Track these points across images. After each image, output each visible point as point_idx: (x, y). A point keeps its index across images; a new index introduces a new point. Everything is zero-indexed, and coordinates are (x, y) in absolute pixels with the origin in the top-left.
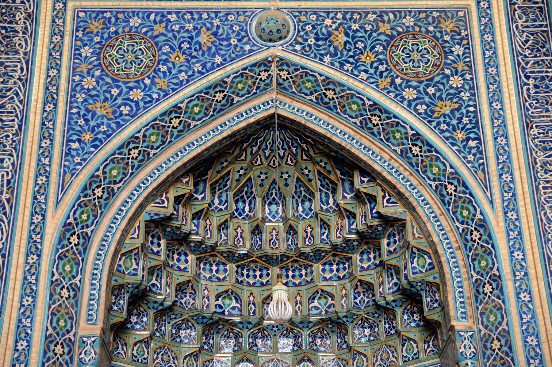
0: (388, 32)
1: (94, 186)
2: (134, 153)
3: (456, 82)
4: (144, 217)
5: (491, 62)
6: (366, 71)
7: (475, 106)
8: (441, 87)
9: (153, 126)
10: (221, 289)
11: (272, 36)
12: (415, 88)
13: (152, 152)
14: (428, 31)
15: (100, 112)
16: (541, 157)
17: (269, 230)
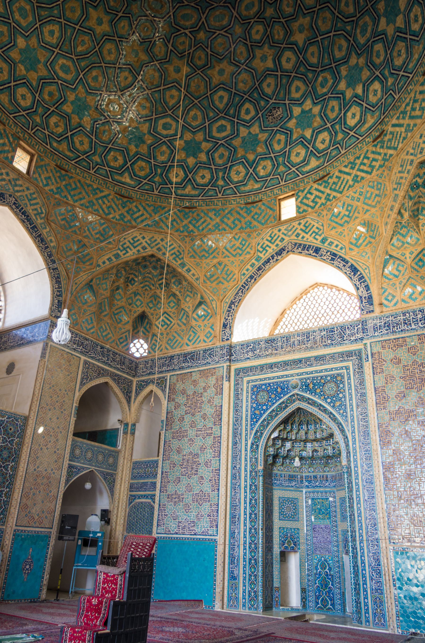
3: (341, 395)
4: (272, 437)
5: (350, 389)
16: (361, 417)
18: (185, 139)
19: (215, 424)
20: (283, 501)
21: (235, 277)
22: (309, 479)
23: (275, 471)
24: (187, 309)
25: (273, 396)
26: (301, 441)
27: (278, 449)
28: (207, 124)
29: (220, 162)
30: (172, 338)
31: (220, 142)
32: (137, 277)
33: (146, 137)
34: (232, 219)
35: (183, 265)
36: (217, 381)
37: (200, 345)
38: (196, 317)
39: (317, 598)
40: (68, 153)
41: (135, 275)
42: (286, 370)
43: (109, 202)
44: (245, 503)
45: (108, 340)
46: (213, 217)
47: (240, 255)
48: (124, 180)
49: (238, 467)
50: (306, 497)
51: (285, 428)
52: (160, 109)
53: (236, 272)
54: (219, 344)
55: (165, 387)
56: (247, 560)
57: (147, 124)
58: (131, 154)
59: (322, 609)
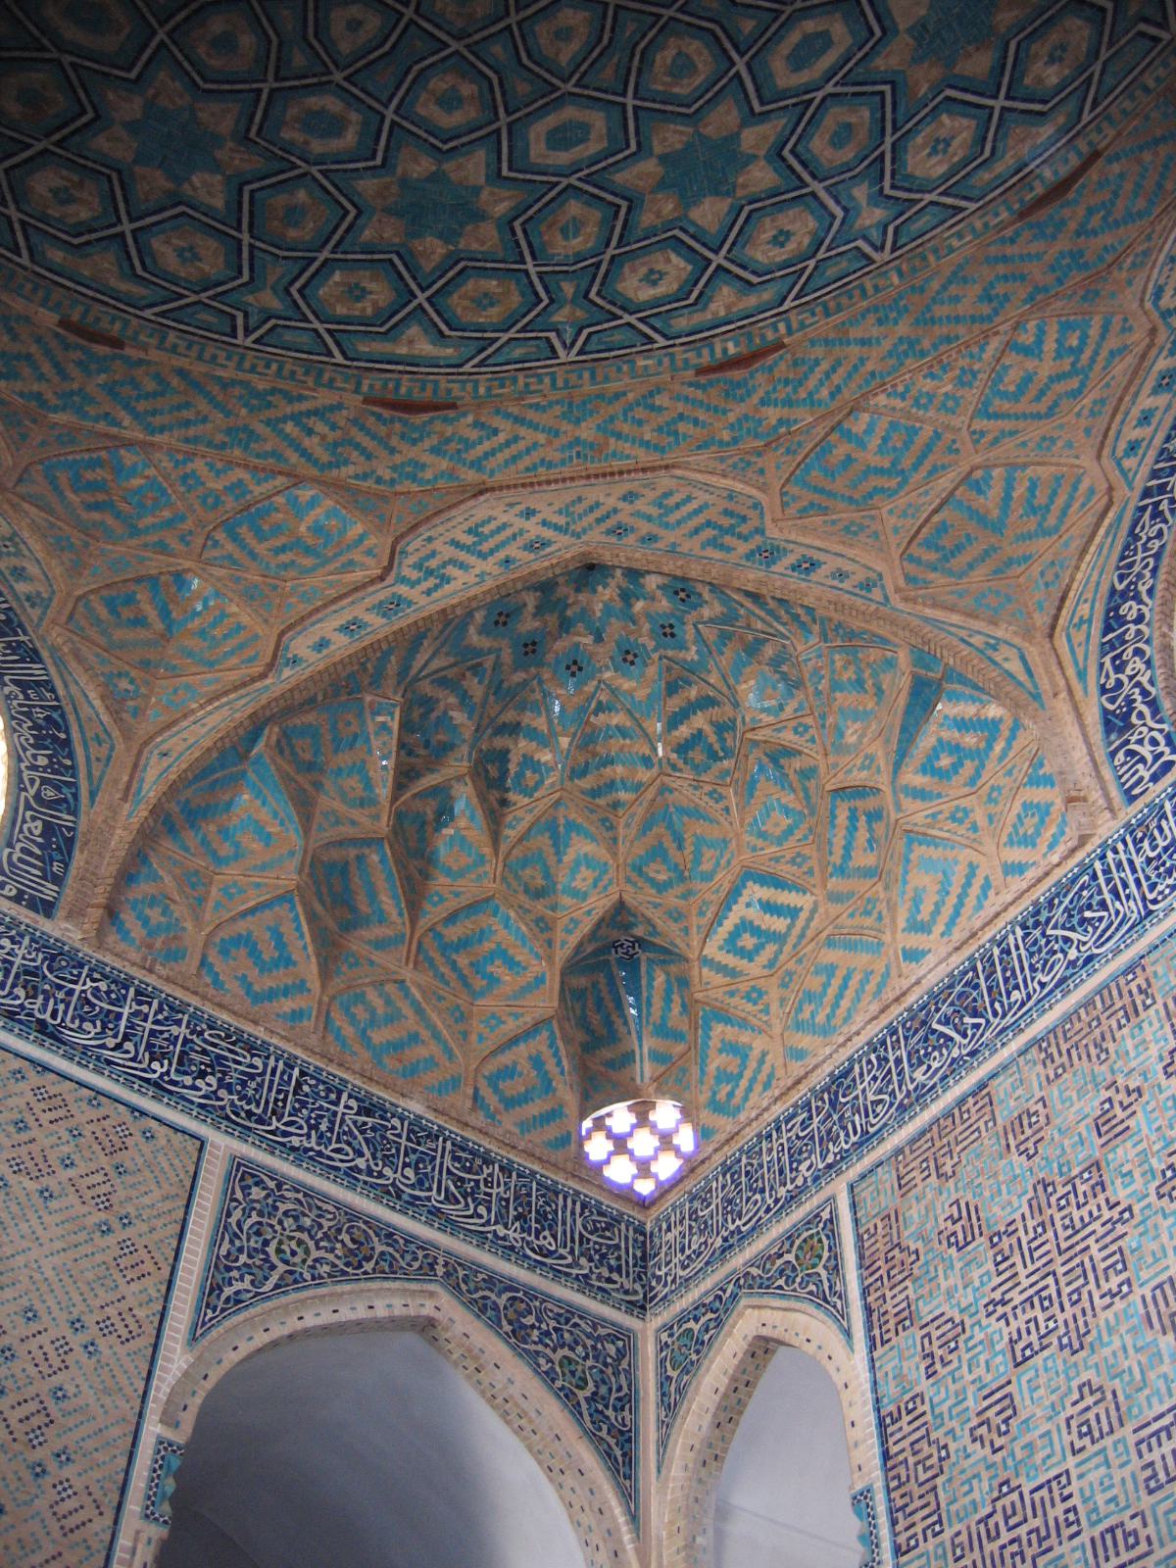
18: (658, 149)
21: (1084, 486)
24: (859, 777)
28: (740, 65)
29: (847, 154)
30: (814, 983)
31: (819, 95)
32: (546, 741)
33: (485, 195)
34: (977, 289)
35: (769, 554)
37: (993, 904)
38: (919, 780)
40: (124, 287)
41: (533, 734)
43: (334, 427)
45: (412, 1071)
46: (875, 331)
47: (1076, 394)
48: (403, 350)
52: (523, 88)
53: (1087, 461)
55: (836, 1269)
57: (481, 155)
58: (428, 266)
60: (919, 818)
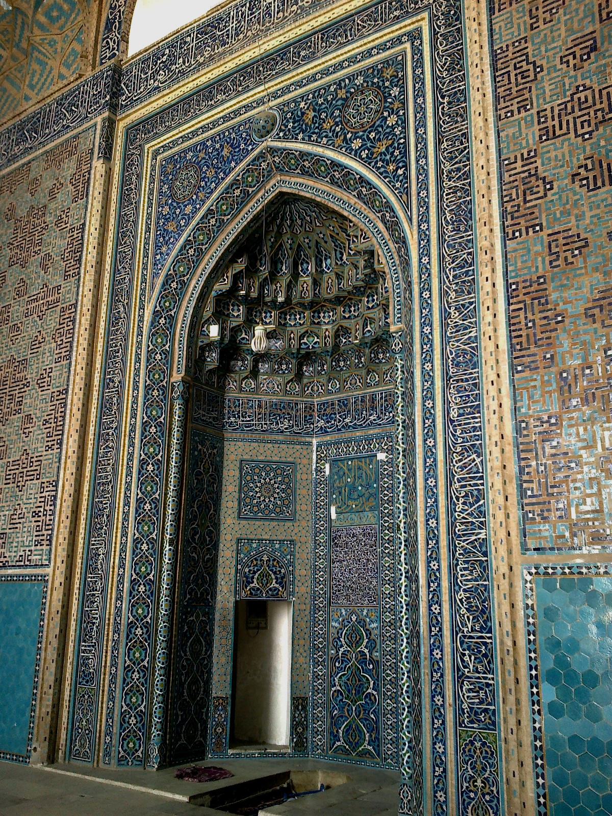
0: (344, 96)
1: (170, 282)
2: (191, 252)
5: (420, 93)
6: (326, 136)
7: (405, 138)
8: (380, 129)
9: (198, 229)
10: (303, 331)
11: (264, 133)
12: (360, 137)
13: (204, 247)
14: (373, 83)
15: (171, 229)
16: (447, 167)
17: (326, 279)
19: (66, 277)
20: (250, 470)
22: (327, 411)
23: (233, 391)
25: (210, 174)
26: (302, 305)
27: (236, 330)
36: (79, 167)
39: (335, 722)
42: (247, 89)
44: (130, 474)
49: (116, 380)
50: (319, 459)
51: (251, 271)
54: (89, 74)
56: (123, 628)
59: (347, 752)
60: (38, 39)
